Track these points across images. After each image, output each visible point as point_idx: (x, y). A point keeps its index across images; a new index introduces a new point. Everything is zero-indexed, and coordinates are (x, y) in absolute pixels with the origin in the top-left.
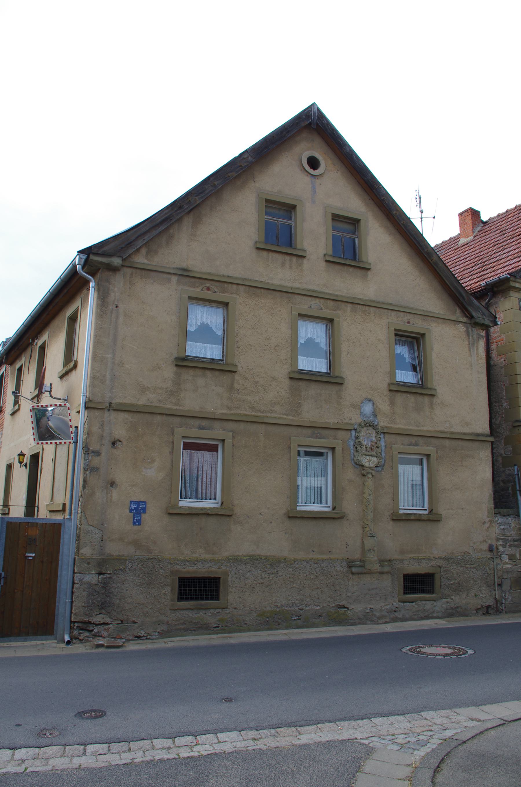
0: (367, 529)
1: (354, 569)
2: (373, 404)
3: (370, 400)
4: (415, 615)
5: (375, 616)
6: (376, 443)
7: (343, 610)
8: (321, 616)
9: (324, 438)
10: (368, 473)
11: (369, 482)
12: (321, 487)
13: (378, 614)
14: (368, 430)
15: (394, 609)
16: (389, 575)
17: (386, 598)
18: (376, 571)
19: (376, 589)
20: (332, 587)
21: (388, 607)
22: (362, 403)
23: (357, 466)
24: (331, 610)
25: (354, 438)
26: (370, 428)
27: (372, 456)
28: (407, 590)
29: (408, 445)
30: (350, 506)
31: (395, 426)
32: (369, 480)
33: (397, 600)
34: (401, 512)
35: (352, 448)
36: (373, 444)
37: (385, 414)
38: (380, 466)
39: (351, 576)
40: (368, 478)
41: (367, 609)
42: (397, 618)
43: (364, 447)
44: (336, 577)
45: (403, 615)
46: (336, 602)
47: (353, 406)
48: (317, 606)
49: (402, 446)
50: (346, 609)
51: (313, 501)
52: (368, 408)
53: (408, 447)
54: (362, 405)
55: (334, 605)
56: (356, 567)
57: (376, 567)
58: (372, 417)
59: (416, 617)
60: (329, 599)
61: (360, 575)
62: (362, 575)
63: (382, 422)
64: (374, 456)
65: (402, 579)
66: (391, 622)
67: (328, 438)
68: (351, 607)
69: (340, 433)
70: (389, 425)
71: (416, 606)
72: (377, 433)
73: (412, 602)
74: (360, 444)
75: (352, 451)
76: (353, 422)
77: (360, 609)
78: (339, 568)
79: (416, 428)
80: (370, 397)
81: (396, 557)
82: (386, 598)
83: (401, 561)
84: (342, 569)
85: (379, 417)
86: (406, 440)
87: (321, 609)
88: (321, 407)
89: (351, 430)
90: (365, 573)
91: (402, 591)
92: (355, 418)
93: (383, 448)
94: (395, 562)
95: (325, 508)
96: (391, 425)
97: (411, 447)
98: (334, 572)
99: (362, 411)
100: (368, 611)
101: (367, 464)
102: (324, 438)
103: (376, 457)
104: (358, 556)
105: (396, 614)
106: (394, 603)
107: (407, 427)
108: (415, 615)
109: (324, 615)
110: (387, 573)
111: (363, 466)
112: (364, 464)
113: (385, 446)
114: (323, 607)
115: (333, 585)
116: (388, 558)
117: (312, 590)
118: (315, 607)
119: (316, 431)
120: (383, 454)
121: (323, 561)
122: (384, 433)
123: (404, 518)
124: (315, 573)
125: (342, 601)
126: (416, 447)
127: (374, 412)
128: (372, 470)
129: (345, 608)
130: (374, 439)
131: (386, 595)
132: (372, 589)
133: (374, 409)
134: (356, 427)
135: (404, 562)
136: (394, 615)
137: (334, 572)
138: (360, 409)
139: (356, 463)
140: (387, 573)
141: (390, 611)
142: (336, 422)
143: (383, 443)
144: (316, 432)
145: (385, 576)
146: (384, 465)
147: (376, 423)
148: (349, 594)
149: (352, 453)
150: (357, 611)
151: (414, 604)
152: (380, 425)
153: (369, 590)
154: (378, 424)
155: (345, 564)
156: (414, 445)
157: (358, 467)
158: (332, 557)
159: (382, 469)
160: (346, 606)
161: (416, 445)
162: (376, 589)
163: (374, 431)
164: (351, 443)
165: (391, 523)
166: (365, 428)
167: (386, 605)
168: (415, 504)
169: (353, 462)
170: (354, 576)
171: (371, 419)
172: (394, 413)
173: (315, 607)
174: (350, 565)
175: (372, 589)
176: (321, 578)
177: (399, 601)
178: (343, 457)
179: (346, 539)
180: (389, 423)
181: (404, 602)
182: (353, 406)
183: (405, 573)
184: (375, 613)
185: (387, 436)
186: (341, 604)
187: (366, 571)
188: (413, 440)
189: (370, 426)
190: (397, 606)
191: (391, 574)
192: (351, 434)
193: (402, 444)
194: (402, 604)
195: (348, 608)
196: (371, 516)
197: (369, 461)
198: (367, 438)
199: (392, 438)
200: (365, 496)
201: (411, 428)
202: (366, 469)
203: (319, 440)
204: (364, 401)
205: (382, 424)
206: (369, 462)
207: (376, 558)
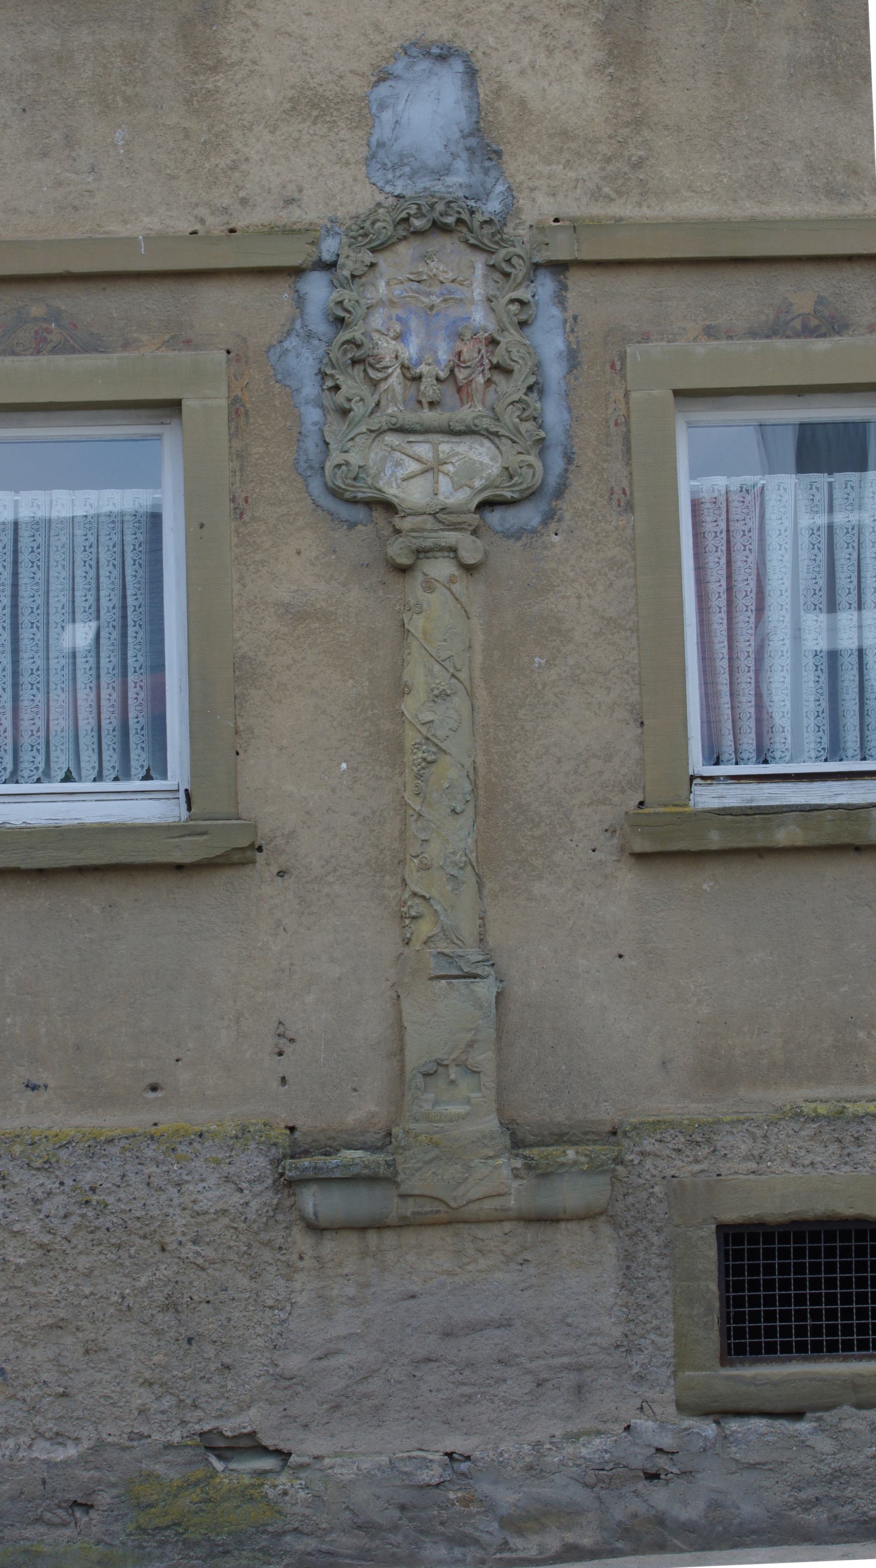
0: (425, 928)
1: (311, 1200)
2: (472, 74)
3: (444, 55)
4: (808, 1505)
5: (489, 1507)
6: (493, 342)
7: (248, 1465)
8: (87, 1507)
9: (87, 349)
10: (421, 553)
11: (438, 605)
12: (861, 652)
13: (506, 1498)
14: (426, 258)
15: (639, 1458)
16: (606, 1230)
17: (579, 1389)
18: (488, 1205)
19: (505, 1323)
20: (163, 1319)
21: (592, 1449)
22: (384, 77)
23: (345, 512)
24: (159, 1468)
25: (320, 327)
26: (448, 244)
27: (451, 432)
28: (749, 1331)
29: (753, 334)
30: (305, 781)
31: (650, 211)
32: (436, 600)
33: (664, 1399)
34: (706, 798)
35: (310, 389)
36: (469, 351)
37: (565, 134)
38: (530, 495)
39: (302, 1241)
40: (429, 587)
41: (427, 1463)
42: (660, 1520)
43: (395, 379)
44: (189, 1250)
45: (714, 1505)
46: (192, 1416)
47: (311, 106)
48: (59, 1438)
49: (700, 349)
50: (269, 1463)
51: (61, 761)
52: (428, 113)
53: (752, 346)
54: (383, 89)
55: (176, 1437)
56: (333, 1182)
57: (496, 1178)
58: (460, 165)
59: (817, 1517)
60: (142, 1397)
61: (372, 1237)
62: (390, 1238)
63: (544, 194)
64: (470, 432)
65: (709, 1255)
66: (613, 1553)
67: (126, 345)
68: (305, 1446)
69: (212, 298)
70: (596, 210)
71: (824, 1444)
72: (500, 272)
73: (797, 1415)
74: (361, 360)
75: (313, 415)
76: (310, 212)
77: (366, 1465)
78: (211, 1195)
79: (825, 208)
80: (441, 31)
81: (668, 1106)
82: (579, 1389)
83: (701, 1135)
84: (237, 1198)
85: (518, 165)
86: (743, 298)
87: (83, 1460)
88: (69, 141)
89: (297, 272)
90: (404, 1224)
91: (710, 1339)
92: (331, 188)
93: (555, 371)
94: (648, 1145)
95: (142, 806)
96: (617, 209)
97: (781, 344)
98: (180, 1221)
99: (383, 131)
100: (426, 1476)
101: (413, 494)
102: (93, 345)
103: (492, 435)
104: (364, 1108)
105: (659, 1497)
106: (644, 1424)
107: (750, 208)
108: (808, 1505)
109: (104, 1499)
110: (587, 1216)
111: (389, 507)
112: (392, 492)
113: (572, 358)
114: (99, 1446)
115: (171, 1306)
116: (605, 1113)
117: (20, 1337)
118: (42, 1451)
119: (37, 304)
120: (554, 413)
121: (96, 1146)
122: (559, 267)
123: (715, 840)
124: (33, 1226)
125: (242, 1408)
126: (821, 345)
127: (476, 131)
128: (455, 527)
129: (264, 1451)
130: (479, 317)
131: (580, 1369)
132: (474, 1328)
133: (476, 109)
134: (329, 248)
135: (721, 1141)
136: (636, 1506)
137: (180, 1221)
138: (364, 116)
139: (335, 493)
140: (587, 1216)
141: (605, 1477)
142: (184, 227)
143: (550, 341)
144: (36, 310)
145: (568, 1240)
146: (560, 492)
147: (493, 206)
148: (293, 1362)
149: (310, 428)
150: (345, 1473)
151: (803, 1426)
152: (529, 216)
153: (447, 1335)
154: (511, 210)
155: (255, 1162)
156: (809, 331)
157: (360, 513)
158: (168, 1119)
159: (549, 516)
160: (268, 1441)
161: (830, 325)
162: (505, 1323)
163: (479, 262)
164: (304, 363)
165: (628, 878)
166: (405, 251)
167: (573, 1437)
168: (728, 741)
169: (316, 486)
170: (329, 1246)
171: (458, 180)
172: (638, 123)
173: (42, 1451)
174: (297, 1163)
175: (474, 1328)
176: (83, 1263)
177: (683, 1408)
178: (241, 456)
179: (291, 997)
180: (596, 195)
181: (722, 1412)
182: (311, 106)
183: (732, 1216)
184: (484, 1487)
185: (580, 284)
186: (229, 1427)
187: (409, 1208)
188: (802, 292)
189: (438, 227)
190: (667, 1441)
191: (617, 1226)
192: (300, 301)
193: (711, 332)
194: (709, 1429)
195: (283, 1455)
196: (450, 838)
197: (431, 469)
198: (425, 313)
199: (626, 299)
200: (409, 706)
201: (782, 208)
202: (406, 524)
203: (60, 360)
204: (399, 67)
205: (539, 207)
206: (430, 476)
207: (490, 1123)
